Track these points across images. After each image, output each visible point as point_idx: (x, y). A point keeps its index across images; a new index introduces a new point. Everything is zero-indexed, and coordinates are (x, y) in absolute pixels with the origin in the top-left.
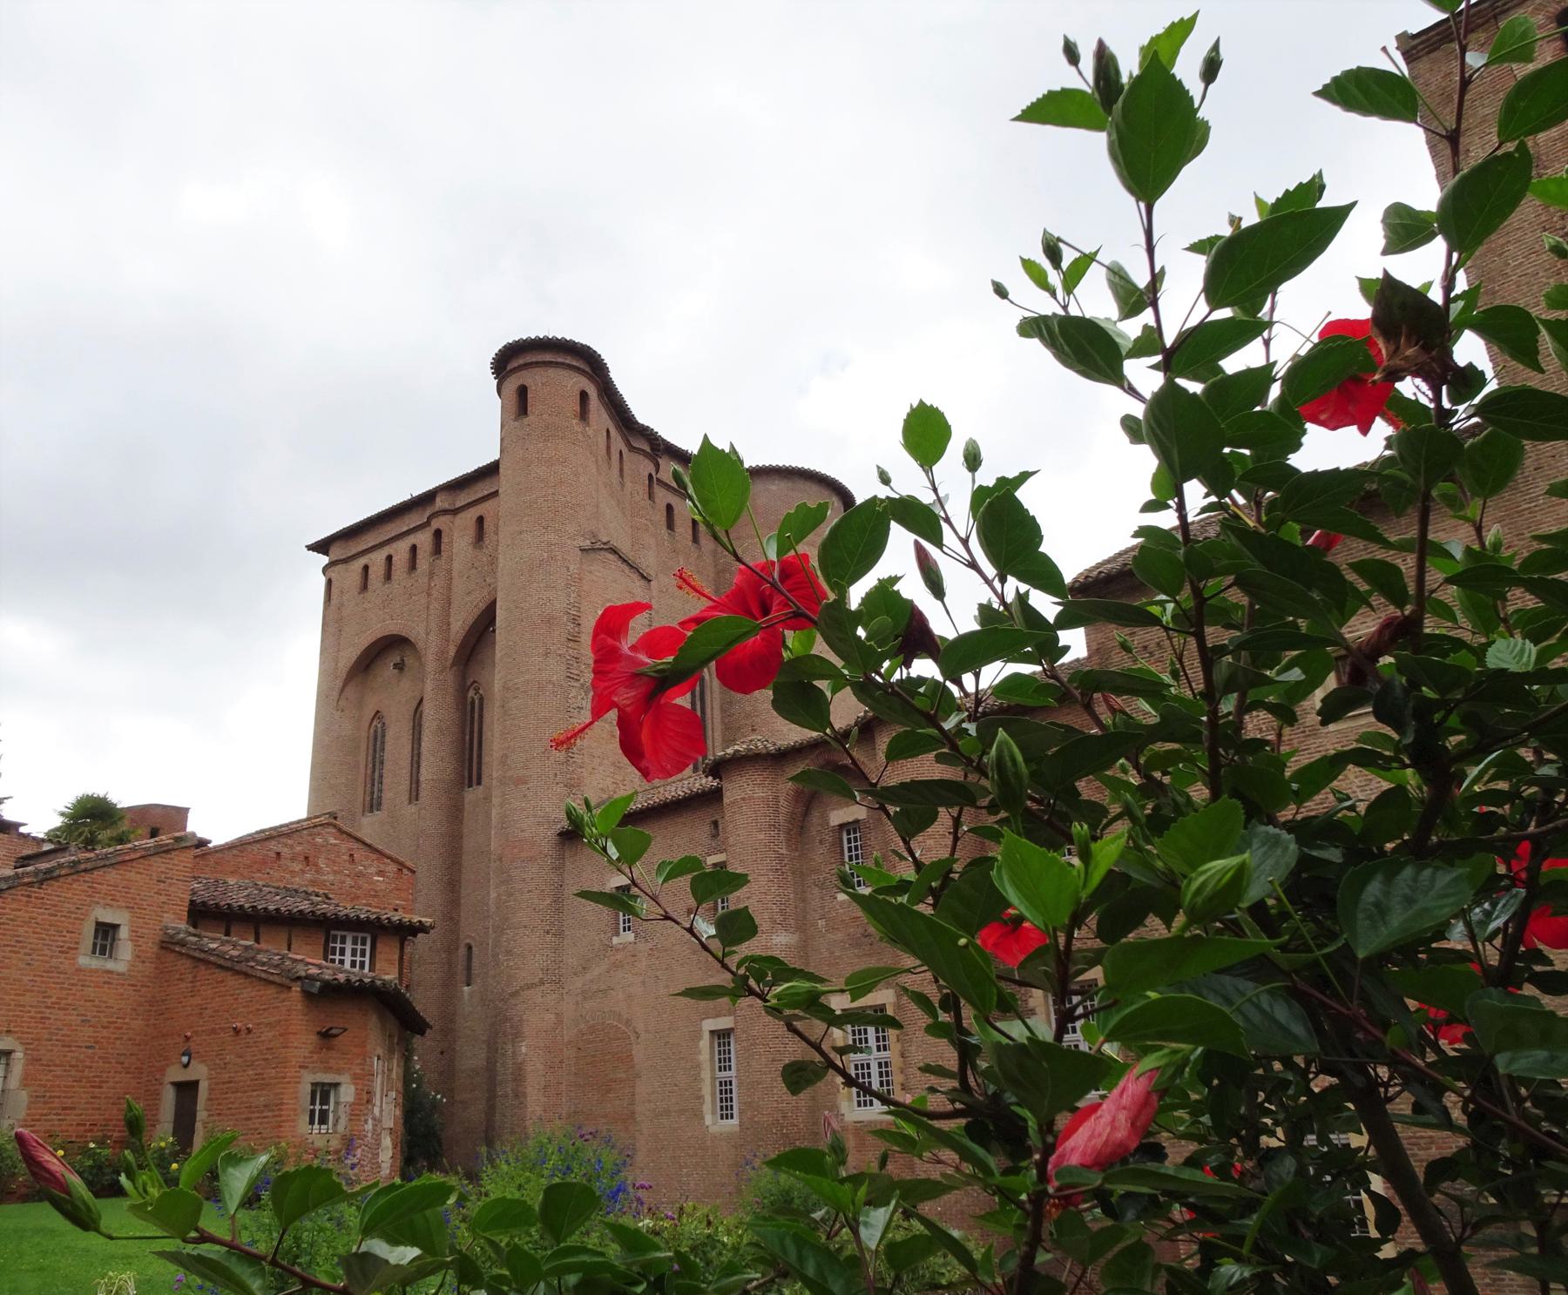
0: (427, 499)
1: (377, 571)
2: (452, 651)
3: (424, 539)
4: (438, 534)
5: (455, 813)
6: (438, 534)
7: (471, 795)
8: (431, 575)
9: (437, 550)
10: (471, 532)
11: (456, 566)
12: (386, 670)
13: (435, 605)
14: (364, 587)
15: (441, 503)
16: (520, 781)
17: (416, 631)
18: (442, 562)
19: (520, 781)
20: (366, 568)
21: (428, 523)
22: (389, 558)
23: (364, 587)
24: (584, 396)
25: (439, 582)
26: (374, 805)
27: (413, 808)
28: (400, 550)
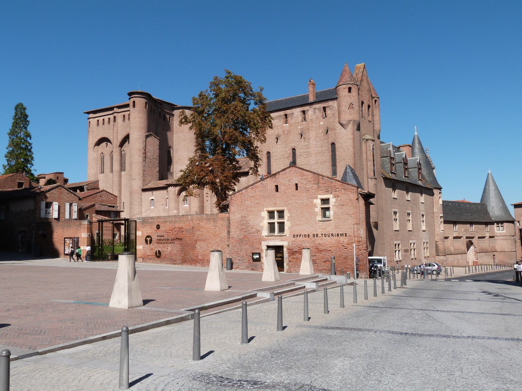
0: (112, 109)
1: (101, 122)
2: (119, 144)
3: (111, 117)
4: (115, 117)
5: (120, 177)
6: (115, 117)
7: (123, 173)
8: (114, 126)
9: (115, 121)
10: (122, 118)
11: (119, 125)
12: (104, 144)
13: (115, 133)
14: (98, 125)
15: (116, 110)
16: (134, 179)
17: (111, 138)
18: (116, 124)
19: (134, 179)
20: (98, 121)
21: (113, 114)
22: (104, 119)
23: (98, 125)
24: (146, 103)
25: (115, 128)
26: (103, 172)
27: (111, 175)
28: (106, 118)
